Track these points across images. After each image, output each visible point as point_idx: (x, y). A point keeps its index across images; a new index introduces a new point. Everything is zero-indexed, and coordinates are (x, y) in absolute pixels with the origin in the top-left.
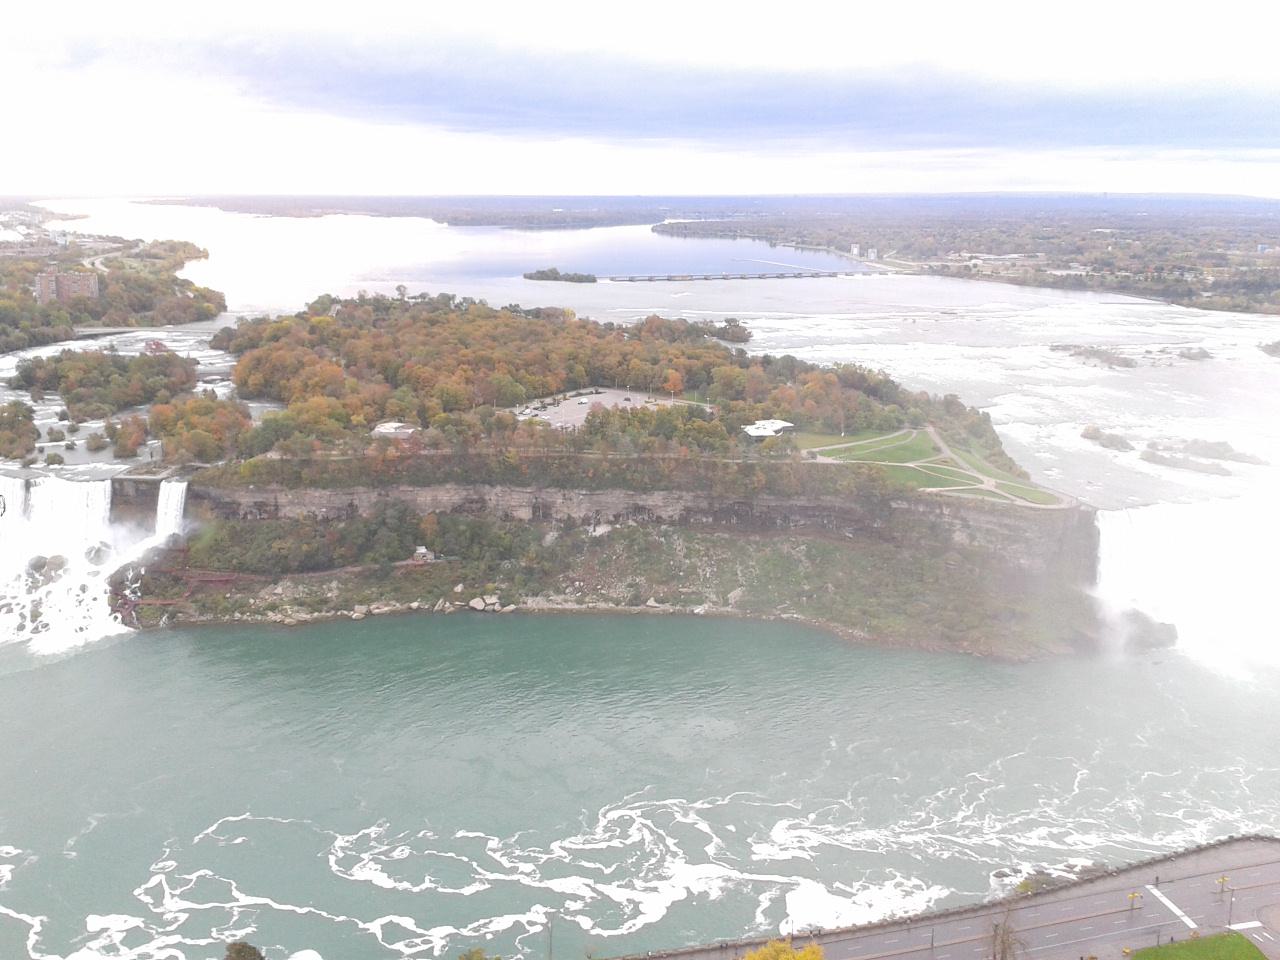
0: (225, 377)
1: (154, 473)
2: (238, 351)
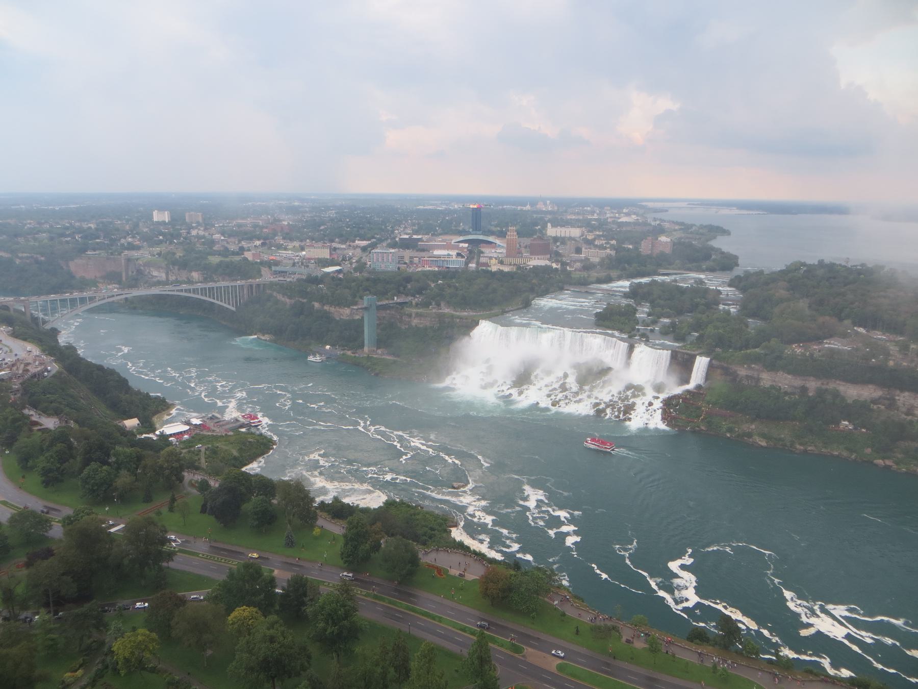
0: (735, 302)
1: (694, 351)
2: (743, 290)
